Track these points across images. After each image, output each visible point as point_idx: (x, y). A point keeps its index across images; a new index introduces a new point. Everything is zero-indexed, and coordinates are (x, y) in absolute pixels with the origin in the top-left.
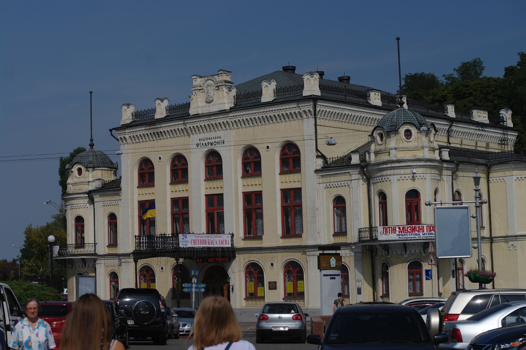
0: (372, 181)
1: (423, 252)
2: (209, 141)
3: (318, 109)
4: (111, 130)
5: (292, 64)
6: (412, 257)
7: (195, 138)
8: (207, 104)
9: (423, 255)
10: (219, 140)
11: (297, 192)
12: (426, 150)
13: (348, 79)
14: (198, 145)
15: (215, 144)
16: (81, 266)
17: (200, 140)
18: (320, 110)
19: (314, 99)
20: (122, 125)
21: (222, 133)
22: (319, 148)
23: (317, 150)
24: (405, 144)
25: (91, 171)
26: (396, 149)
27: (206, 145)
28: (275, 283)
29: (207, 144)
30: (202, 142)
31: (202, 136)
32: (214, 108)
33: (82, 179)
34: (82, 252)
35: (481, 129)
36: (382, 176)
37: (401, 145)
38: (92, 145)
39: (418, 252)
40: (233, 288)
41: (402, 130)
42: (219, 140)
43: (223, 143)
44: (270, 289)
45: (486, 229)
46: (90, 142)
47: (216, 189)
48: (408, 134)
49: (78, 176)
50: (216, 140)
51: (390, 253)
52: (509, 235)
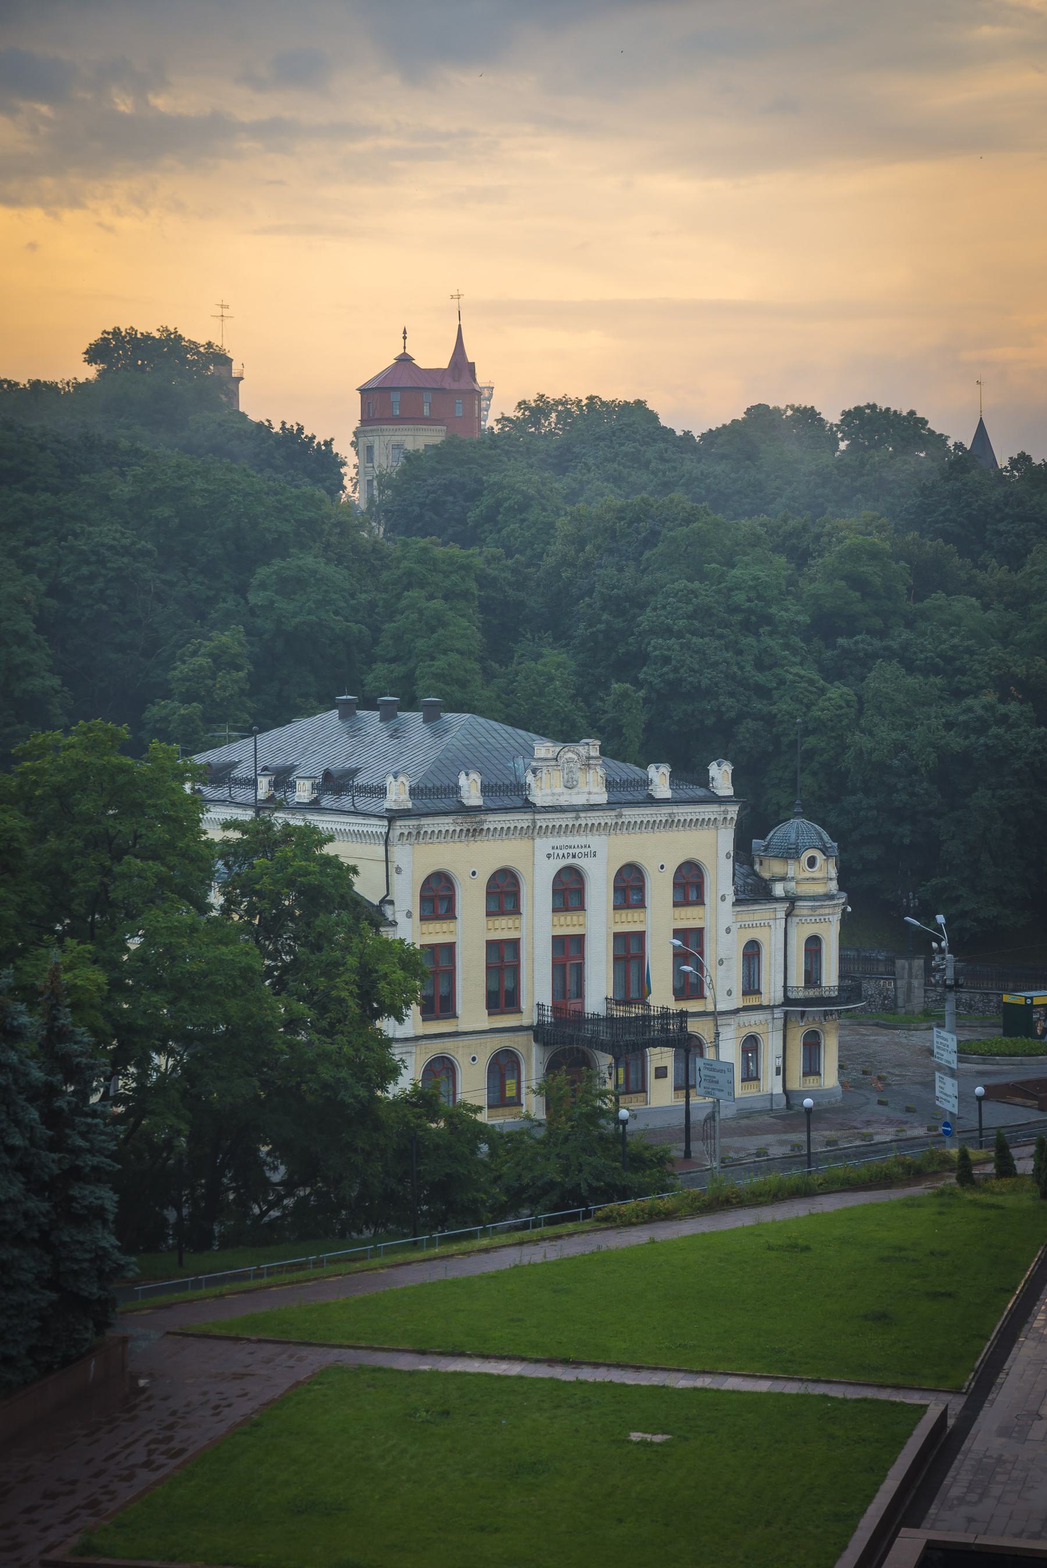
2: (571, 851)
7: (544, 844)
8: (566, 790)
10: (587, 850)
11: (698, 934)
14: (549, 856)
15: (580, 855)
17: (553, 848)
20: (387, 810)
21: (596, 841)
27: (563, 856)
29: (566, 856)
30: (557, 851)
31: (562, 841)
32: (579, 800)
42: (587, 850)
43: (595, 855)
44: (657, 1077)
47: (564, 927)
50: (583, 850)
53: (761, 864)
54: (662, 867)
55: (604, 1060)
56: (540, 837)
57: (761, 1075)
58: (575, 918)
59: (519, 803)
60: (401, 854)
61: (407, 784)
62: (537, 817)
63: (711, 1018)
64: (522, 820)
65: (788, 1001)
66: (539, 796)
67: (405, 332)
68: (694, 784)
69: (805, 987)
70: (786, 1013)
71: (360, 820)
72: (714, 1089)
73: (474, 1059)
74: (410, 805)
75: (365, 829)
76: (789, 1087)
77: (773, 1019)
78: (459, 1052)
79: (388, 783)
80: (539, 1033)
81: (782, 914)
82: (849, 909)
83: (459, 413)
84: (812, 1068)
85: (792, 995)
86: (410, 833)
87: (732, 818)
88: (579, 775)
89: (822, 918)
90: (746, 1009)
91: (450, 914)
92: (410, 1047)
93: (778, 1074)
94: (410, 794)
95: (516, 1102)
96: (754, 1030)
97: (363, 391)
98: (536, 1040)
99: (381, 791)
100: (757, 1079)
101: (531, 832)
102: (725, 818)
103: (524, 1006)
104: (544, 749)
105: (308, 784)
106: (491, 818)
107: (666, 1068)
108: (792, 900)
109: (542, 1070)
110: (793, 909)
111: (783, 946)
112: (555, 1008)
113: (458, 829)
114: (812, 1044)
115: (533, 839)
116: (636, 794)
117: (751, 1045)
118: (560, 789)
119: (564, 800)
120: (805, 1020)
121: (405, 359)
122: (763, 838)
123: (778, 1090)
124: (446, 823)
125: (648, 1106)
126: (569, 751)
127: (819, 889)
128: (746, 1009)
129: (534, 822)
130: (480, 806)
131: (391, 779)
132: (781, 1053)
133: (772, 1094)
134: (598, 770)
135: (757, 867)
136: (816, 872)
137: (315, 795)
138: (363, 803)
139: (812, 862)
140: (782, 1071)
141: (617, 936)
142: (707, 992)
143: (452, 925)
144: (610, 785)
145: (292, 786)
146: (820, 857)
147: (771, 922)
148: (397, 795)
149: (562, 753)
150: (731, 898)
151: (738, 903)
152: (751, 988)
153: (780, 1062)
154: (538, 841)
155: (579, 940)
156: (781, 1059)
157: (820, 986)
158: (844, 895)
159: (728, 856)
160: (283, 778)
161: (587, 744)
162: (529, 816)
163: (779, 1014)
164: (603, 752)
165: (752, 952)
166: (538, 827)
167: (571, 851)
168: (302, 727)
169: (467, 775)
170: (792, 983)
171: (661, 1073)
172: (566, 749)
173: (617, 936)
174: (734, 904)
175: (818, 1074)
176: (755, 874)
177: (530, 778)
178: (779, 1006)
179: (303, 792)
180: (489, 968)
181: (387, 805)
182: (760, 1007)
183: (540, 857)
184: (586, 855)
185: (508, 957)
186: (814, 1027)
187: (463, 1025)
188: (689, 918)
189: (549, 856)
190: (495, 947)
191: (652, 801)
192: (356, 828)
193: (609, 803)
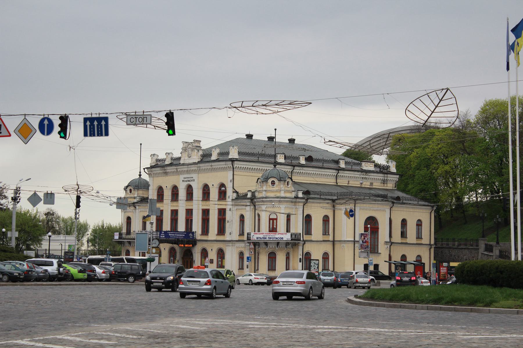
0: (256, 206)
1: (277, 247)
2: (188, 179)
3: (235, 166)
4: (144, 169)
5: (251, 133)
6: (271, 250)
7: (182, 177)
8: (188, 158)
9: (277, 249)
10: (192, 179)
12: (283, 192)
13: (294, 140)
14: (183, 181)
16: (128, 245)
18: (236, 167)
19: (233, 160)
22: (234, 188)
23: (233, 188)
24: (271, 189)
25: (136, 191)
26: (265, 191)
28: (213, 260)
32: (191, 161)
33: (132, 196)
34: (130, 238)
35: (365, 174)
36: (259, 205)
37: (269, 189)
38: (140, 175)
39: (273, 247)
40: (194, 262)
41: (270, 181)
42: (192, 179)
45: (330, 236)
46: (139, 173)
48: (273, 183)
49: (130, 193)
51: (260, 247)
52: (342, 240)
106: (168, 168)
113: (162, 172)
155: (191, 210)
167: (188, 179)
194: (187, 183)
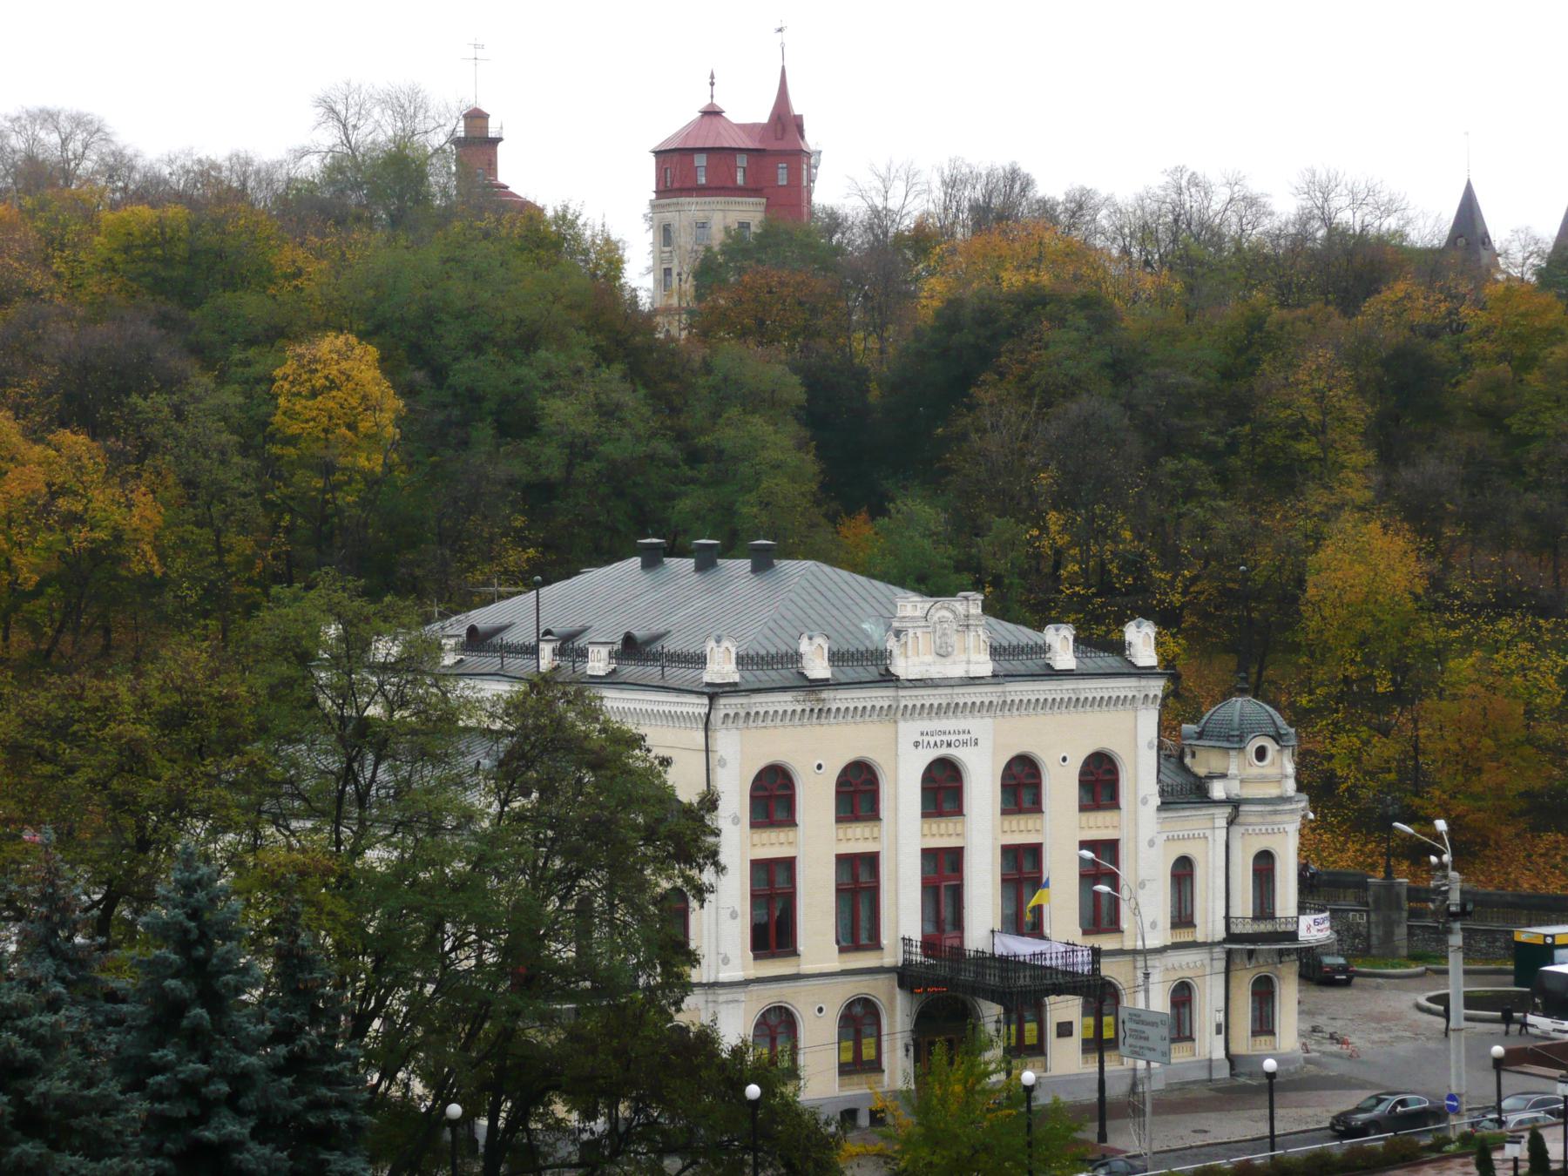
0: (1236, 831)
2: (945, 738)
7: (910, 730)
10: (966, 737)
11: (1108, 849)
14: (917, 744)
17: (922, 734)
20: (708, 685)
21: (979, 726)
27: (932, 744)
30: (926, 739)
32: (957, 671)
42: (966, 737)
43: (976, 744)
50: (961, 737)
53: (1194, 755)
54: (1064, 759)
55: (991, 1012)
56: (905, 720)
57: (1197, 1035)
58: (951, 825)
59: (873, 672)
60: (727, 742)
61: (733, 650)
62: (902, 693)
63: (1128, 958)
64: (880, 697)
65: (1231, 937)
66: (903, 667)
67: (712, 77)
68: (1105, 651)
69: (1255, 918)
70: (1229, 953)
71: (672, 698)
72: (1142, 1048)
73: (820, 1010)
74: (736, 678)
75: (679, 710)
76: (1234, 1049)
77: (1212, 960)
78: (801, 1001)
79: (708, 650)
80: (906, 976)
81: (1223, 823)
82: (1311, 816)
83: (783, 180)
84: (1264, 1025)
85: (1237, 929)
86: (737, 714)
87: (1155, 696)
88: (954, 639)
89: (1276, 827)
90: (1176, 946)
91: (1036, 807)
92: (740, 994)
93: (1218, 1032)
94: (737, 663)
95: (875, 1066)
96: (1185, 974)
97: (659, 154)
98: (901, 985)
99: (699, 660)
100: (1191, 1038)
101: (890, 714)
102: (1147, 696)
103: (885, 941)
104: (911, 605)
105: (604, 651)
106: (842, 694)
107: (1071, 1023)
108: (1235, 804)
109: (909, 1026)
110: (1235, 817)
111: (1224, 864)
112: (929, 945)
113: (799, 708)
114: (1264, 992)
115: (896, 722)
116: (1029, 663)
117: (1182, 995)
118: (930, 658)
119: (937, 670)
120: (1253, 961)
121: (712, 113)
122: (1194, 720)
123: (1219, 1054)
124: (784, 702)
125: (1048, 1074)
126: (942, 608)
127: (1272, 791)
128: (1176, 946)
129: (896, 699)
130: (827, 680)
131: (711, 644)
132: (1222, 1004)
133: (1210, 1060)
134: (980, 633)
135: (1188, 760)
136: (1265, 768)
137: (613, 666)
138: (677, 674)
139: (1261, 754)
140: (1225, 1029)
141: (1006, 850)
142: (1124, 925)
143: (791, 834)
144: (996, 652)
145: (583, 654)
146: (1272, 747)
147: (1208, 833)
148: (721, 667)
149: (932, 611)
150: (1157, 801)
151: (1165, 805)
152: (1183, 917)
153: (1221, 1017)
154: (902, 725)
156: (1222, 1015)
157: (1272, 917)
158: (1304, 797)
159: (1150, 746)
160: (570, 646)
161: (966, 598)
162: (890, 692)
163: (1219, 952)
164: (987, 609)
165: (1183, 871)
166: (902, 707)
167: (945, 738)
168: (594, 580)
169: (810, 638)
170: (1236, 912)
171: (1065, 1030)
172: (938, 605)
173: (1006, 850)
174: (1159, 809)
175: (1272, 1033)
176: (1186, 770)
177: (891, 644)
178: (1219, 943)
179: (598, 663)
180: (840, 891)
181: (707, 678)
182: (1194, 945)
183: (905, 745)
184: (965, 743)
185: (864, 878)
186: (1265, 971)
187: (807, 967)
188: (1100, 826)
189: (917, 744)
190: (847, 862)
191: (1052, 673)
192: (667, 708)
193: (994, 676)
194: (929, 755)
